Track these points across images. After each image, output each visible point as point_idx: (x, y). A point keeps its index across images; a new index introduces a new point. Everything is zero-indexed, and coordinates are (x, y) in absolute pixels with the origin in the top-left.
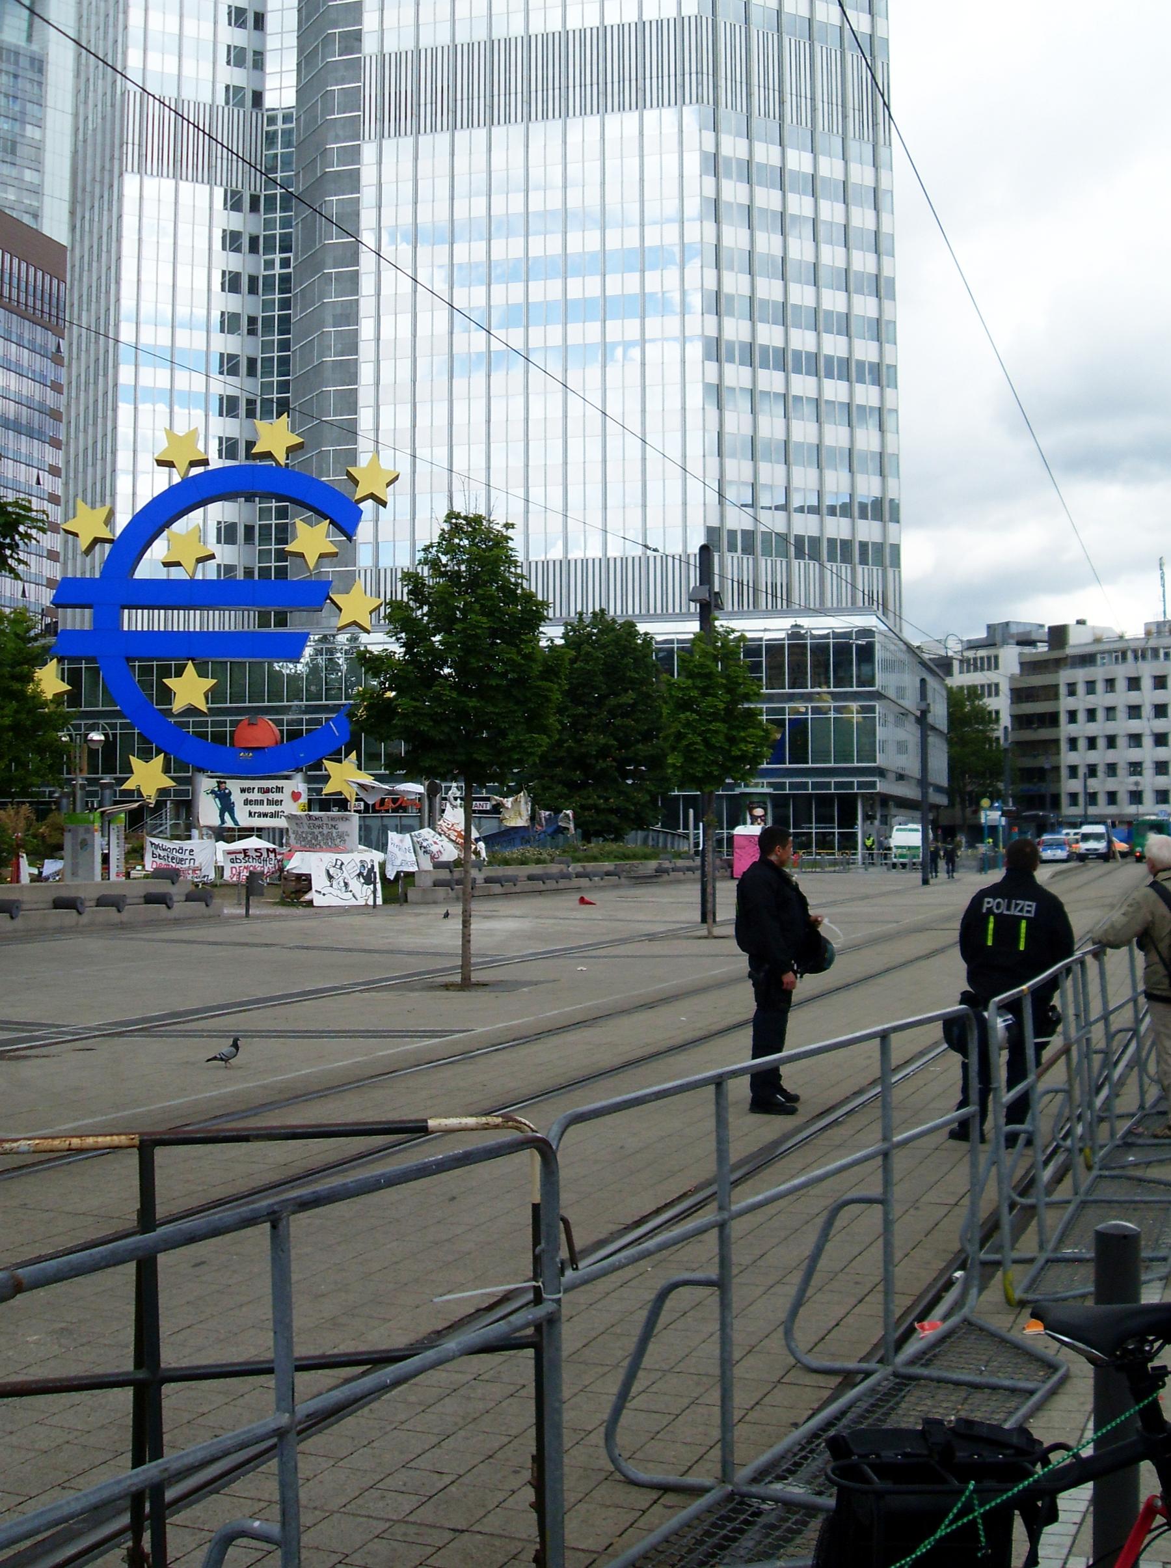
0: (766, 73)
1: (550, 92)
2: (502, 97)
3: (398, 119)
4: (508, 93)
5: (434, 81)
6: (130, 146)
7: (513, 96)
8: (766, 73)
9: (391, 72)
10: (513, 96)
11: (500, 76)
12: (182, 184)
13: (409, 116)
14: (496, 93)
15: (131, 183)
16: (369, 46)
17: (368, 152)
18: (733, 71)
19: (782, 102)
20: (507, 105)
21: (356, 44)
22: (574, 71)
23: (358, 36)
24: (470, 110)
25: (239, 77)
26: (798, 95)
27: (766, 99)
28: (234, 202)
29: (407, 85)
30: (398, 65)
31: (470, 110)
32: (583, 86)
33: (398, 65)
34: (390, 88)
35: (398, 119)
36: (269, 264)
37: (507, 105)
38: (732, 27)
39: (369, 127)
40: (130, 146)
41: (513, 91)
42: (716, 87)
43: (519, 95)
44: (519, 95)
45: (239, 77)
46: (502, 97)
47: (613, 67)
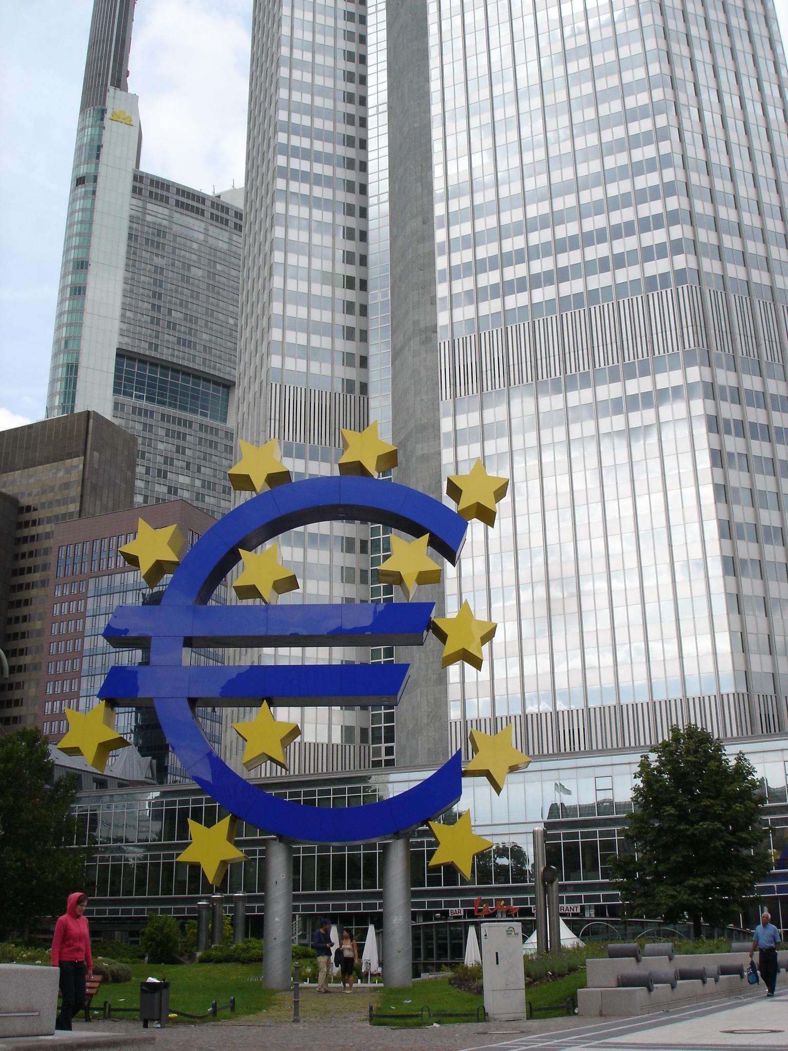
0: (744, 326)
1: (580, 352)
2: (544, 360)
3: (466, 383)
4: (548, 356)
6: (273, 421)
7: (552, 358)
8: (744, 326)
10: (552, 358)
14: (539, 357)
21: (433, 335)
23: (434, 329)
25: (352, 373)
26: (770, 341)
27: (747, 344)
29: (472, 359)
32: (605, 344)
34: (459, 362)
35: (466, 383)
38: (716, 293)
39: (446, 390)
40: (273, 421)
41: (552, 354)
43: (557, 357)
44: (557, 357)
45: (352, 373)
46: (544, 360)
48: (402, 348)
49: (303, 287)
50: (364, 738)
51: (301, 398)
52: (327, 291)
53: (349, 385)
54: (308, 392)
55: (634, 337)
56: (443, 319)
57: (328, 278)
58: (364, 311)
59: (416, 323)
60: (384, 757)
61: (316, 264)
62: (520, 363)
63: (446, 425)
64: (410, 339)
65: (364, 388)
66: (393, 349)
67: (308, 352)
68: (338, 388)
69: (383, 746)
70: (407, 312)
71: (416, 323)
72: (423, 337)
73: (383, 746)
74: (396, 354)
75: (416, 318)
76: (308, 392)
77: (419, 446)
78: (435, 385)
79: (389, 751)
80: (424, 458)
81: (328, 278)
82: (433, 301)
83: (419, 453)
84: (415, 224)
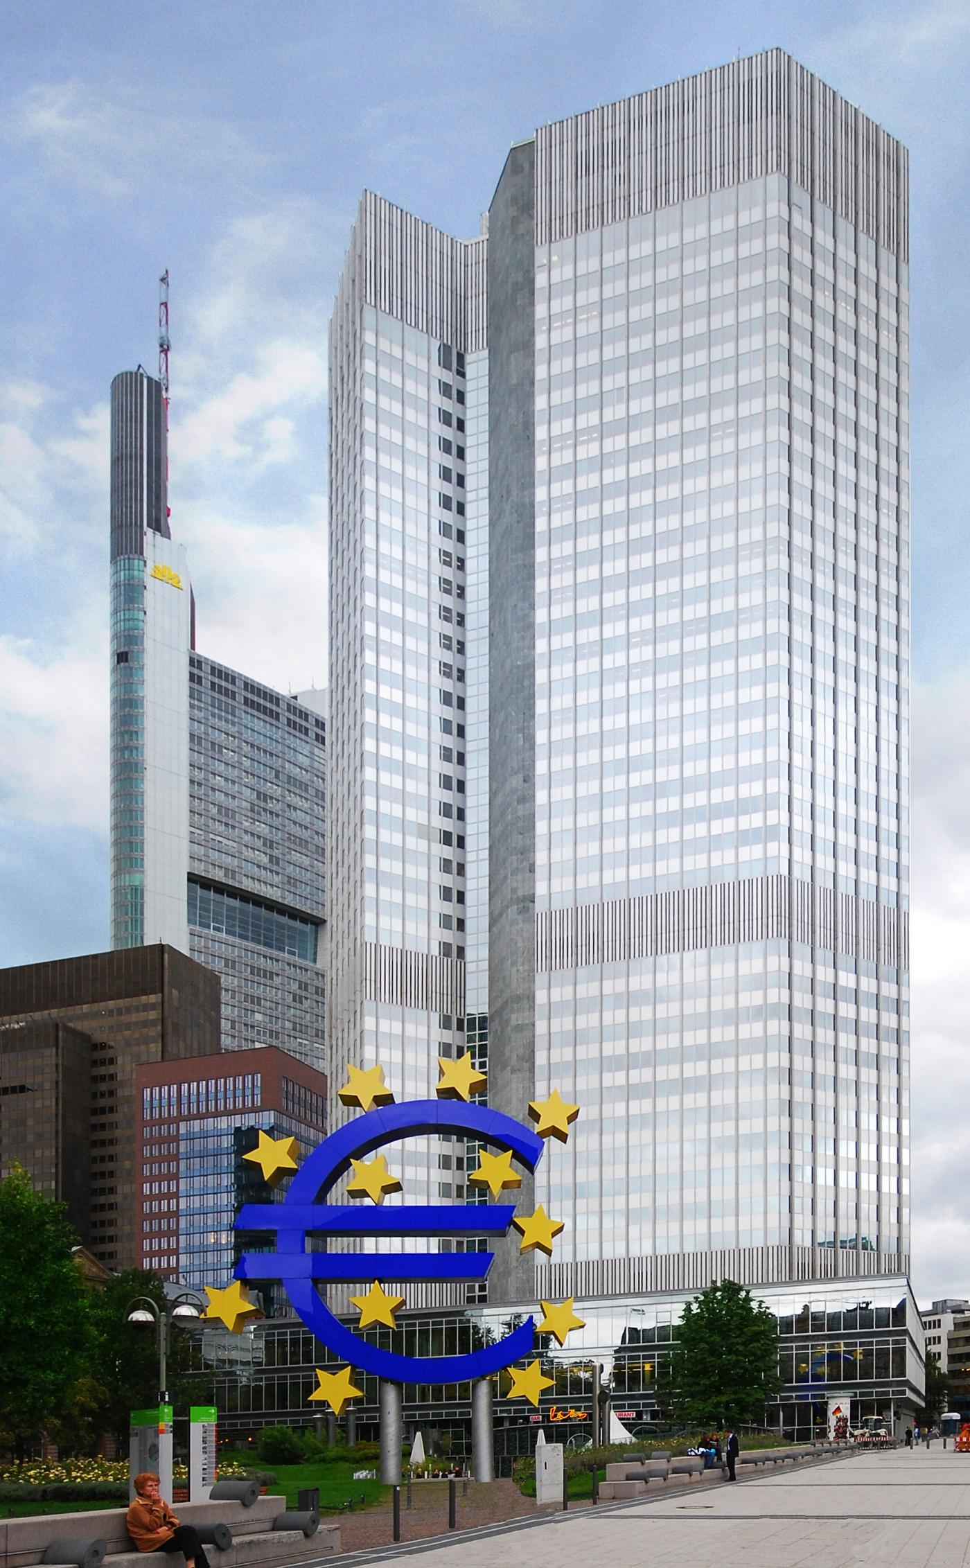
3: (562, 957)
12: (406, 1009)
13: (568, 953)
16: (540, 907)
17: (541, 979)
25: (449, 936)
28: (446, 1023)
29: (568, 933)
30: (562, 919)
33: (562, 919)
34: (556, 935)
35: (562, 957)
39: (541, 963)
48: (500, 915)
49: (397, 839)
51: (397, 959)
52: (423, 845)
53: (446, 949)
56: (541, 889)
57: (424, 832)
58: (461, 869)
59: (514, 890)
61: (411, 814)
63: (541, 997)
64: (507, 907)
65: (461, 951)
66: (491, 913)
68: (435, 951)
70: (505, 877)
71: (514, 890)
72: (521, 906)
74: (493, 921)
75: (515, 885)
76: (404, 953)
77: (514, 1017)
78: (531, 956)
80: (519, 1028)
81: (424, 832)
82: (532, 869)
83: (514, 1022)
84: (516, 781)
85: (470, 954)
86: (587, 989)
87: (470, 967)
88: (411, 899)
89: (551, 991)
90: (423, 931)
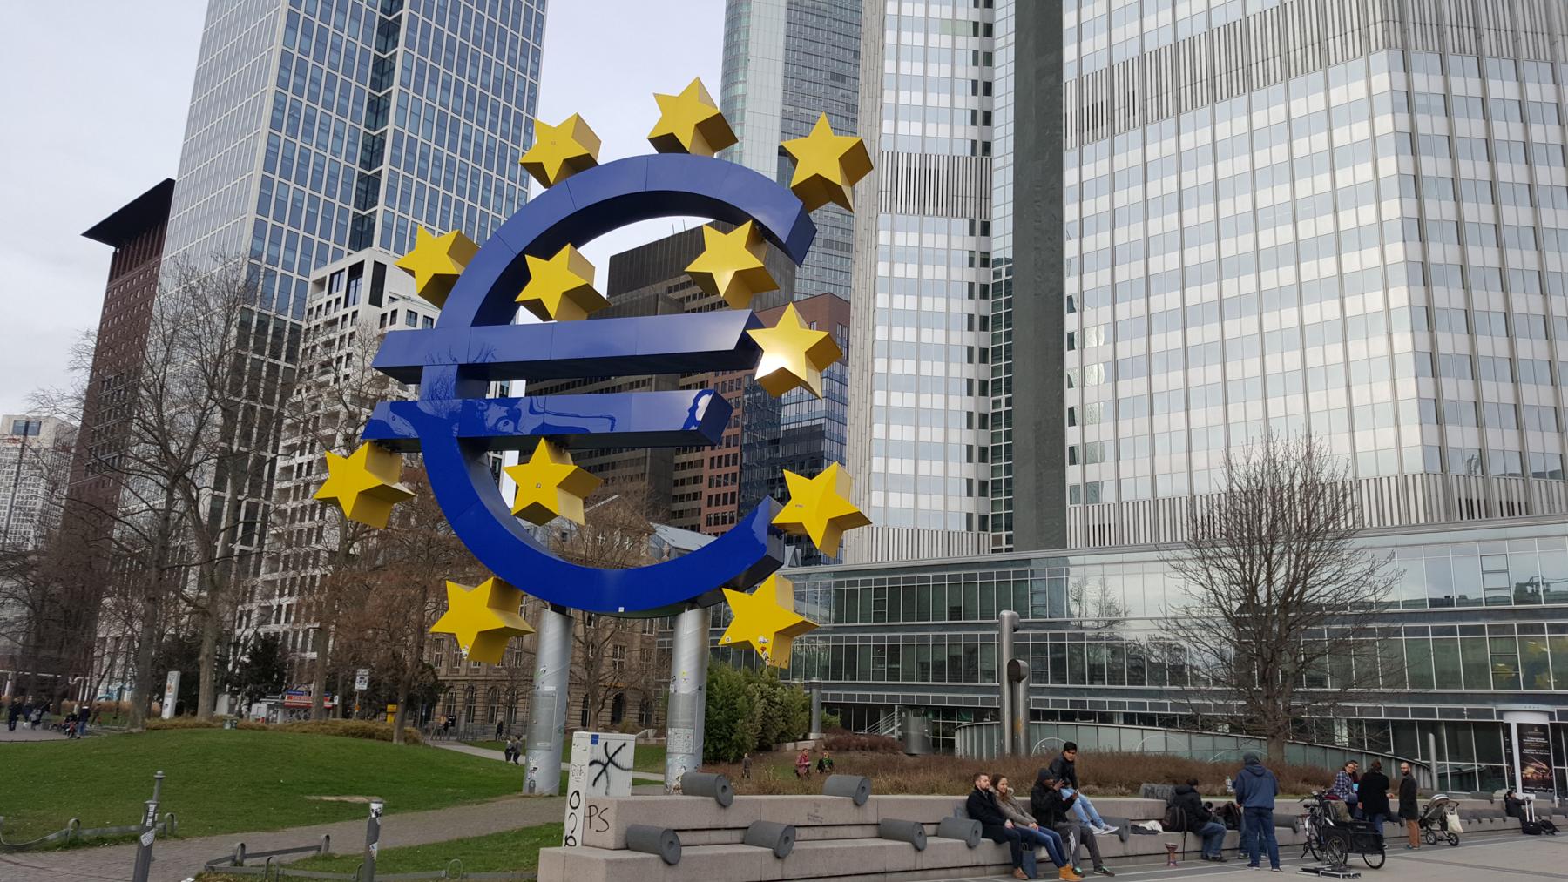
0: (1459, 14)
5: (1126, 86)
8: (1459, 14)
9: (1088, 89)
11: (1185, 72)
13: (1103, 120)
15: (884, 218)
16: (1069, 74)
17: (1070, 157)
18: (1422, 16)
19: (1478, 38)
20: (1193, 93)
22: (1256, 53)
24: (1159, 104)
29: (1103, 96)
31: (1159, 104)
32: (1265, 60)
34: (1088, 102)
35: (1095, 126)
36: (997, 274)
37: (1193, 93)
39: (1070, 141)
42: (1404, 31)
47: (1294, 39)
50: (983, 527)
54: (924, 157)
55: (1304, 47)
56: (1069, 53)
60: (1004, 546)
62: (1160, 95)
65: (987, 148)
67: (924, 113)
69: (1004, 534)
73: (1004, 534)
76: (924, 157)
79: (1009, 539)
85: (997, 149)
86: (1128, 158)
87: (997, 163)
88: (932, 99)
89: (1083, 168)
90: (944, 130)
